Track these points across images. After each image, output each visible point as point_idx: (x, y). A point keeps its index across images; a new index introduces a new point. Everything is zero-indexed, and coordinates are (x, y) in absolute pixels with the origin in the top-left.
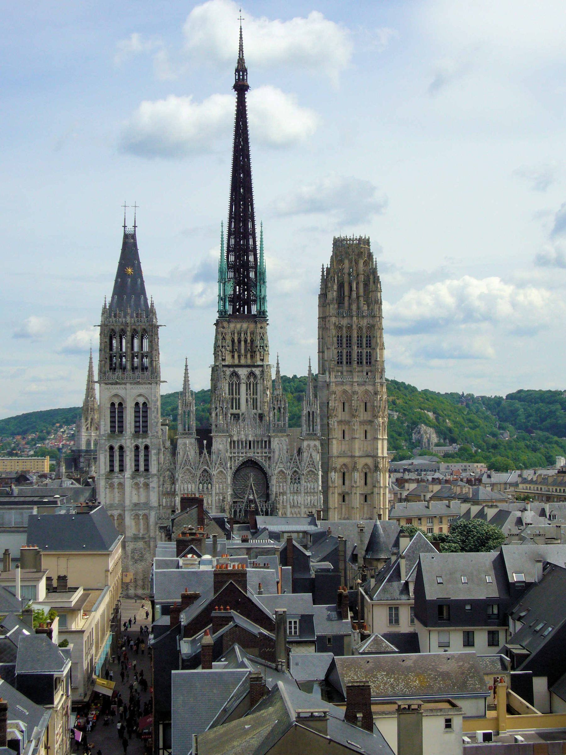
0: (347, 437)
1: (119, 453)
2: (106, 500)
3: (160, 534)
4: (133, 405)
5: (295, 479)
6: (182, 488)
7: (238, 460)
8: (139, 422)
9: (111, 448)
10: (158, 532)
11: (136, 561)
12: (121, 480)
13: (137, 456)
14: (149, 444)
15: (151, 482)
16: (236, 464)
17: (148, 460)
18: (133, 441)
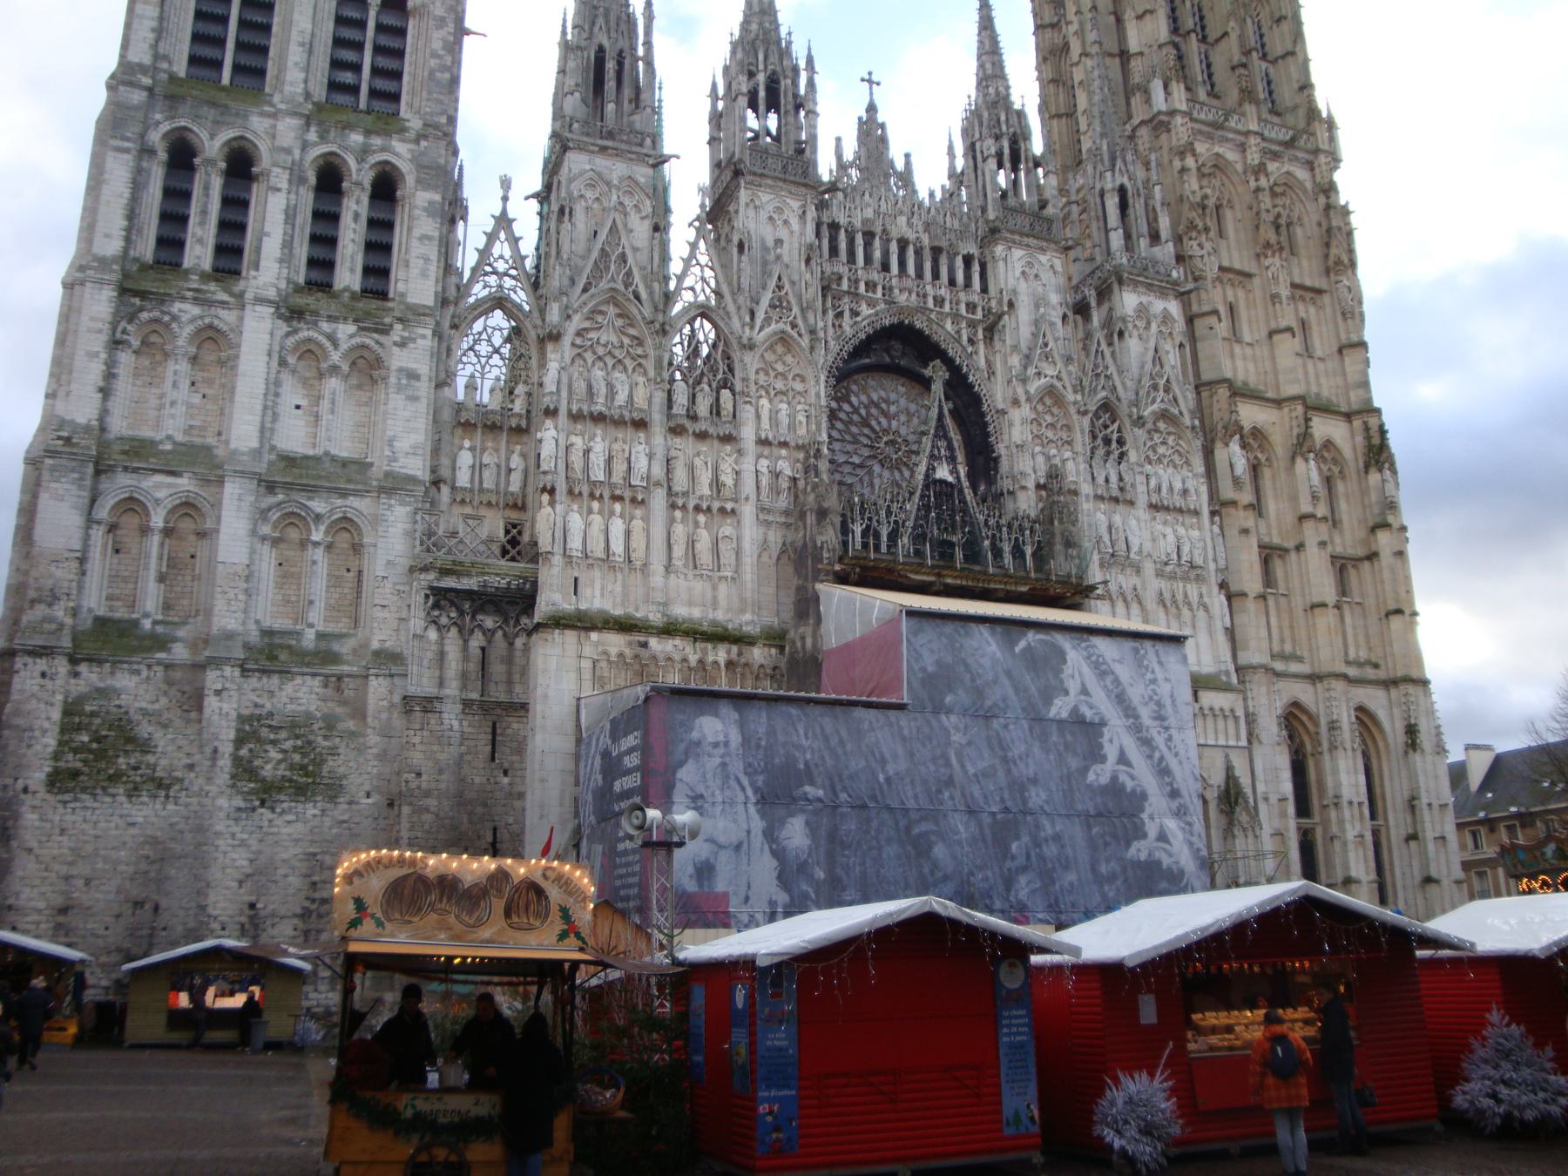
1: (226, 186)
2: (104, 413)
3: (433, 635)
5: (1107, 441)
6: (580, 386)
7: (855, 313)
8: (357, 68)
9: (182, 156)
10: (417, 623)
11: (266, 793)
12: (223, 313)
13: (326, 217)
14: (405, 166)
15: (402, 344)
16: (848, 330)
17: (386, 249)
18: (312, 136)
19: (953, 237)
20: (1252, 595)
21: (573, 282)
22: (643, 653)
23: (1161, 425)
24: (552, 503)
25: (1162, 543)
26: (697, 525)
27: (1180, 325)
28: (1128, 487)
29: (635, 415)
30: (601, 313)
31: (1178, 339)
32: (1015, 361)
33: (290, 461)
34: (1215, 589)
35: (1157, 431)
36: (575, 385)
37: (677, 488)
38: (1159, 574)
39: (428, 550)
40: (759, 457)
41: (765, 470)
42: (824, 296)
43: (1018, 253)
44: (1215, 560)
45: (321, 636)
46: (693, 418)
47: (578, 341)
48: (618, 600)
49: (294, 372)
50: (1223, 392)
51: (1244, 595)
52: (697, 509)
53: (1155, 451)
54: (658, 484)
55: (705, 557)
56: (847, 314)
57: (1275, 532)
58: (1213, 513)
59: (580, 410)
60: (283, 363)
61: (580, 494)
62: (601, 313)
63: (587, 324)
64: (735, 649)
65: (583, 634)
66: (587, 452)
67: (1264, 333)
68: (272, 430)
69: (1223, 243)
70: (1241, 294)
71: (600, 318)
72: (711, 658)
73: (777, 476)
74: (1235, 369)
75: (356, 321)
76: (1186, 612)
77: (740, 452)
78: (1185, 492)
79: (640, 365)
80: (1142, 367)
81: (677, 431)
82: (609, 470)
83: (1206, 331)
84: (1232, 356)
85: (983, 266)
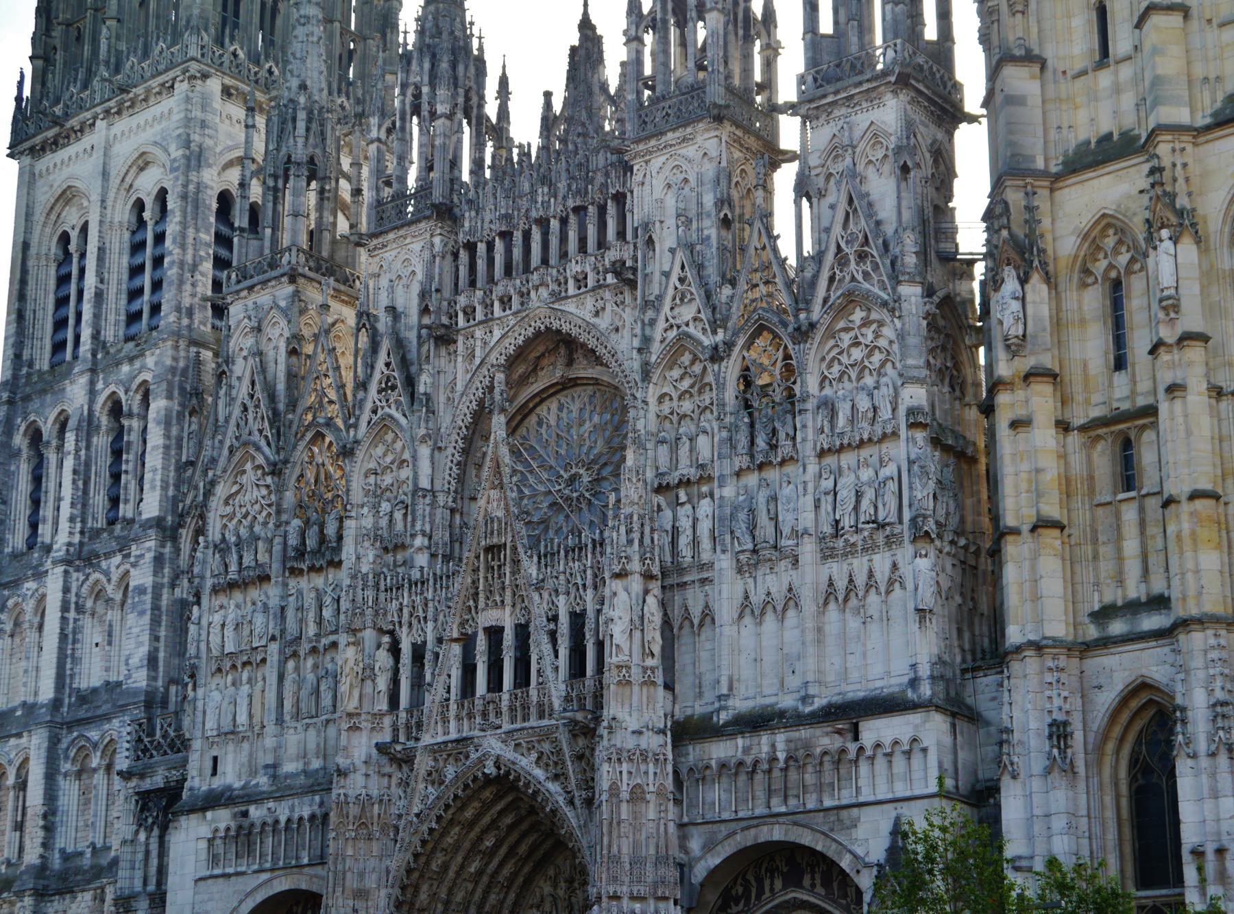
0: (1121, 42)
4: (122, 213)
13: (117, 453)
22: (246, 822)
23: (858, 316)
24: (194, 689)
25: (827, 505)
33: (84, 698)
34: (909, 549)
38: (827, 554)
39: (138, 758)
43: (657, 162)
45: (95, 850)
47: (229, 509)
49: (93, 615)
51: (1016, 532)
53: (840, 363)
54: (273, 638)
56: (478, 352)
60: (80, 609)
62: (244, 472)
64: (317, 798)
65: (200, 814)
66: (223, 625)
68: (72, 676)
72: (296, 816)
75: (120, 551)
76: (873, 598)
78: (875, 409)
81: (295, 572)
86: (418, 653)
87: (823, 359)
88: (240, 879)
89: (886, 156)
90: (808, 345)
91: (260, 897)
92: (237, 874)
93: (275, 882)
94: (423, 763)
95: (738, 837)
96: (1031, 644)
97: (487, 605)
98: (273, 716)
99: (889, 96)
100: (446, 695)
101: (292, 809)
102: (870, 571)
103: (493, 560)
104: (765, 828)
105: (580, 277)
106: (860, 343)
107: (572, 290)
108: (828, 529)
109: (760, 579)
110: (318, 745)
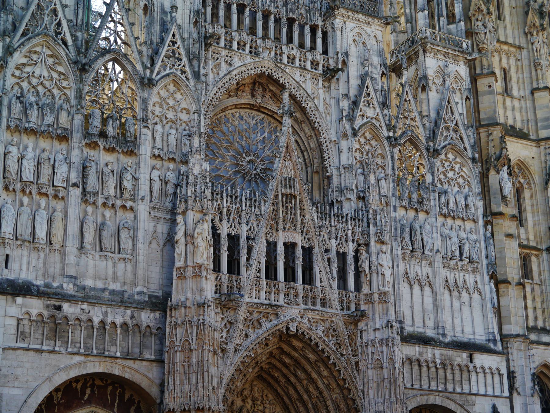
19: (302, 11)
20: (513, 283)
21: (15, 28)
23: (451, 156)
25: (449, 242)
26: (103, 215)
27: (466, 83)
28: (425, 202)
29: (59, 132)
30: (36, 52)
31: (466, 94)
32: (345, 104)
34: (487, 278)
35: (447, 160)
36: (13, 107)
37: (89, 189)
40: (153, 168)
41: (157, 179)
42: (207, 50)
43: (350, 25)
44: (487, 257)
46: (103, 135)
48: (40, 273)
50: (497, 132)
51: (509, 283)
52: (105, 204)
54: (75, 185)
55: (109, 242)
56: (223, 65)
57: (532, 237)
58: (487, 223)
59: (17, 126)
61: (14, 190)
63: (24, 61)
64: (129, 312)
65: (9, 297)
66: (21, 158)
67: (528, 92)
69: (501, 24)
70: (513, 61)
71: (35, 57)
72: (109, 320)
73: (166, 183)
74: (506, 117)
76: (464, 294)
77: (138, 164)
78: (467, 206)
79: (65, 94)
80: (438, 113)
81: (93, 145)
82: (38, 175)
83: (487, 89)
84: (505, 107)
85: (325, 34)
86: (234, 240)
87: (438, 169)
88: (52, 356)
89: (460, 89)
90: (435, 160)
91: (73, 374)
92: (49, 352)
93: (88, 365)
94: (243, 313)
95: (418, 399)
96: (518, 336)
97: (284, 228)
98: (77, 242)
99: (462, 63)
100: (258, 274)
101: (106, 314)
102: (465, 281)
103: (287, 203)
104: (432, 397)
105: (292, 57)
106: (454, 170)
107: (285, 60)
108: (449, 254)
109: (412, 266)
110: (114, 273)
